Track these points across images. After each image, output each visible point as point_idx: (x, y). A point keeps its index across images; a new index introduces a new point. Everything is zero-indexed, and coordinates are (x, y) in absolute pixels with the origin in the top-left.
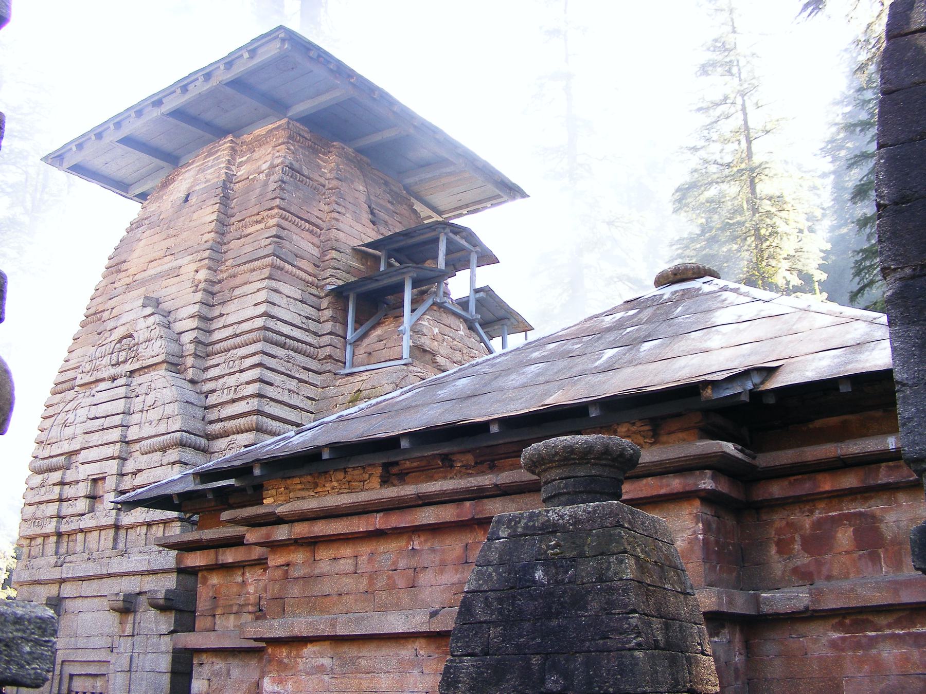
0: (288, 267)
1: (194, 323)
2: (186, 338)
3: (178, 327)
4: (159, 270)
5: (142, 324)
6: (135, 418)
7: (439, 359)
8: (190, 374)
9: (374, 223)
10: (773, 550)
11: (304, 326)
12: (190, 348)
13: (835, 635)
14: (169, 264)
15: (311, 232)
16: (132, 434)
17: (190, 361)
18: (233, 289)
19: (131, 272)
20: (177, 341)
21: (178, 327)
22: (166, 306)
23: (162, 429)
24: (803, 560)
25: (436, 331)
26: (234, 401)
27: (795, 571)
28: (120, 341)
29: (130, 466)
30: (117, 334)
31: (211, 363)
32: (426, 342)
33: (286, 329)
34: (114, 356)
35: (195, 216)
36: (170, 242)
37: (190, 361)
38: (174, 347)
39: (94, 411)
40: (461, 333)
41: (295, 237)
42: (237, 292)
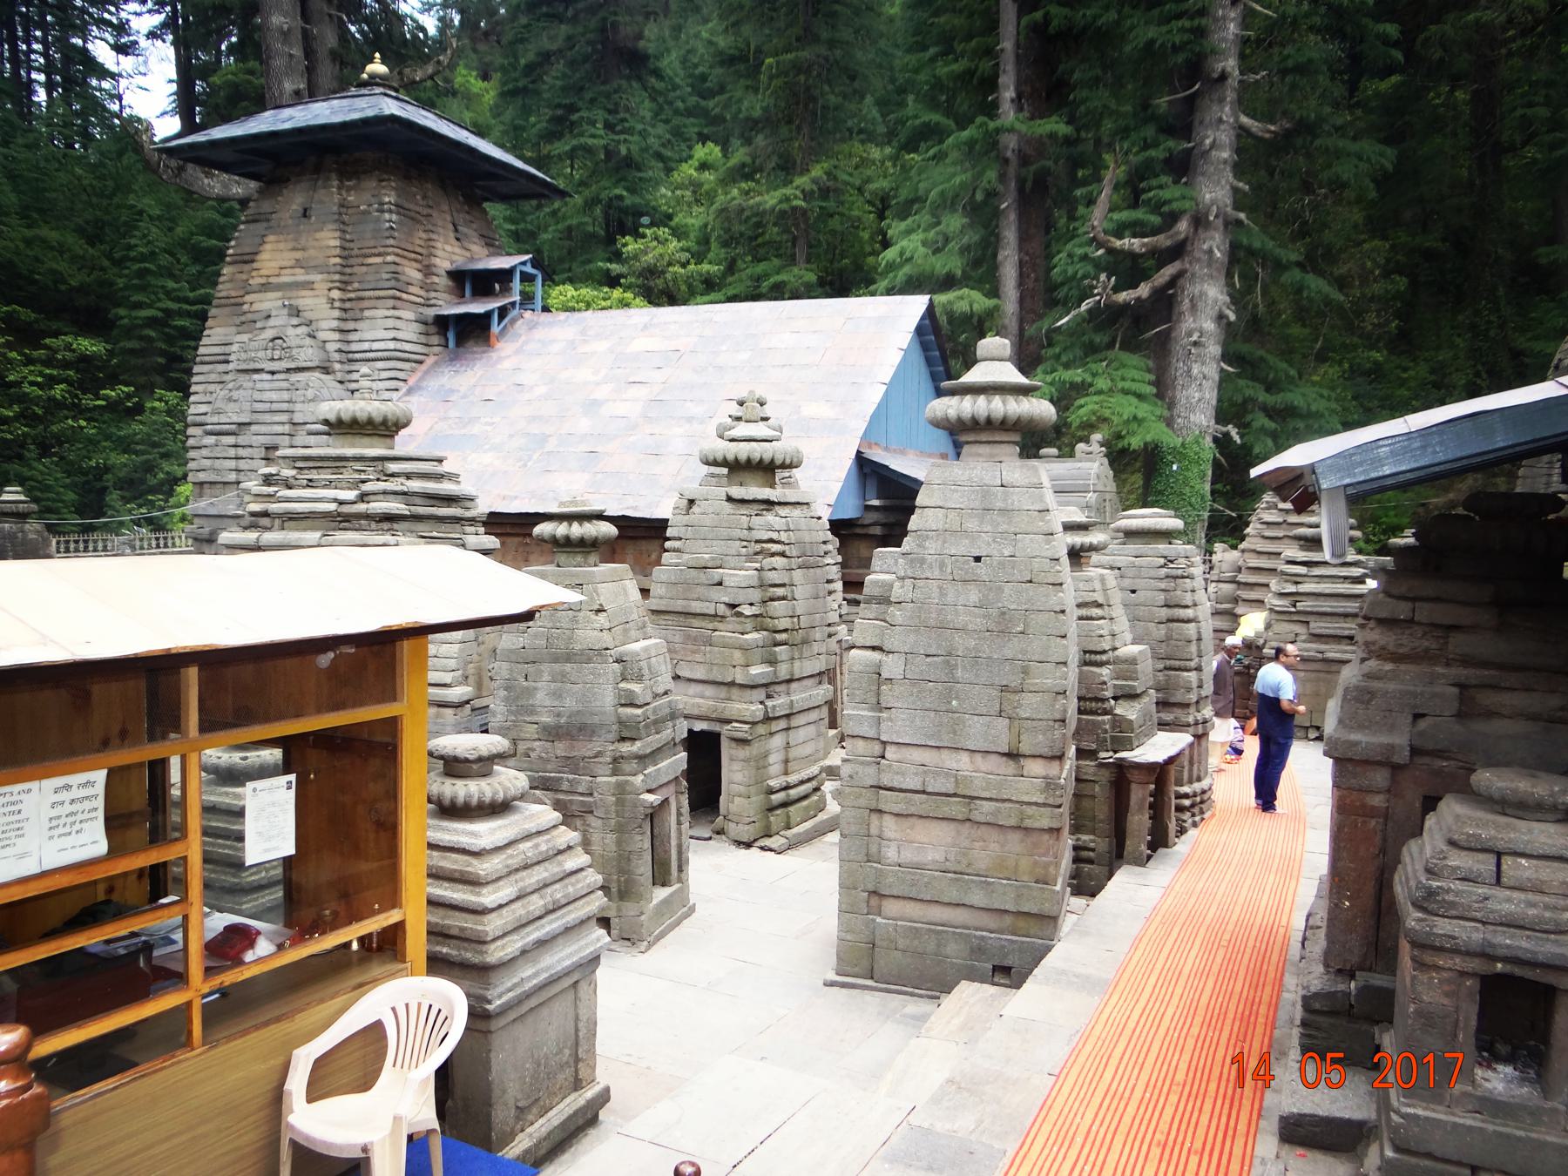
0: (404, 296)
1: (336, 336)
2: (331, 347)
3: (322, 335)
5: (291, 332)
6: (298, 407)
8: (339, 376)
9: (458, 239)
12: (337, 356)
14: (301, 276)
15: (416, 260)
16: (298, 418)
17: (337, 366)
18: (362, 310)
19: (263, 272)
20: (323, 348)
21: (322, 335)
22: (308, 315)
28: (273, 340)
29: (298, 440)
30: (269, 334)
33: (408, 347)
34: (269, 352)
35: (318, 235)
36: (299, 255)
37: (337, 366)
38: (322, 355)
39: (257, 396)
42: (367, 313)
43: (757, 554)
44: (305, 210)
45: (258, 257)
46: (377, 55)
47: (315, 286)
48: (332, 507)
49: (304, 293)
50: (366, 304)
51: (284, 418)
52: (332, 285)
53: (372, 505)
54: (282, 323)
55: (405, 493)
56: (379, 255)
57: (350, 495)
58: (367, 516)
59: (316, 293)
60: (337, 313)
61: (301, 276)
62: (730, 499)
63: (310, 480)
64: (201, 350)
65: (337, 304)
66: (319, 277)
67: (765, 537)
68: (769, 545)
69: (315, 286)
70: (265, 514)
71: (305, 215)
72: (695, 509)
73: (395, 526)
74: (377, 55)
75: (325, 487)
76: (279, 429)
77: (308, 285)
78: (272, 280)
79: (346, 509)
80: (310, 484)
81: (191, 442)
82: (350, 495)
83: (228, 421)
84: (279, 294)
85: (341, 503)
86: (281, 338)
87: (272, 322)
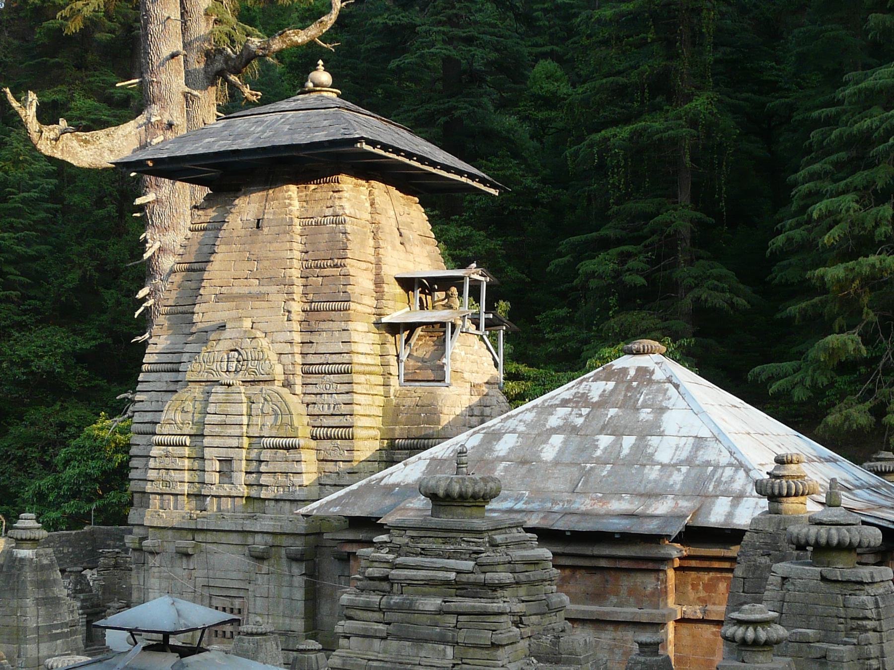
4: (246, 290)
7: (466, 375)
10: (690, 587)
11: (372, 352)
13: (714, 630)
19: (217, 282)
24: (702, 594)
25: (463, 353)
26: (332, 415)
27: (699, 598)
30: (224, 345)
31: (309, 381)
32: (458, 366)
40: (476, 347)
41: (360, 280)
42: (323, 326)
43: (852, 629)
44: (259, 220)
45: (209, 267)
46: (320, 62)
47: (271, 297)
48: (452, 576)
49: (258, 304)
50: (323, 315)
53: (489, 575)
55: (509, 563)
56: (336, 266)
57: (469, 565)
58: (484, 585)
61: (254, 286)
62: (824, 579)
63: (423, 549)
66: (275, 288)
67: (861, 615)
68: (865, 622)
69: (271, 297)
70: (385, 579)
71: (258, 227)
72: (788, 586)
73: (506, 593)
74: (320, 62)
75: (439, 556)
76: (234, 442)
77: (260, 297)
78: (224, 290)
79: (464, 578)
80: (424, 552)
81: (134, 451)
82: (469, 565)
83: (179, 432)
85: (459, 572)
86: (236, 350)
87: (227, 334)
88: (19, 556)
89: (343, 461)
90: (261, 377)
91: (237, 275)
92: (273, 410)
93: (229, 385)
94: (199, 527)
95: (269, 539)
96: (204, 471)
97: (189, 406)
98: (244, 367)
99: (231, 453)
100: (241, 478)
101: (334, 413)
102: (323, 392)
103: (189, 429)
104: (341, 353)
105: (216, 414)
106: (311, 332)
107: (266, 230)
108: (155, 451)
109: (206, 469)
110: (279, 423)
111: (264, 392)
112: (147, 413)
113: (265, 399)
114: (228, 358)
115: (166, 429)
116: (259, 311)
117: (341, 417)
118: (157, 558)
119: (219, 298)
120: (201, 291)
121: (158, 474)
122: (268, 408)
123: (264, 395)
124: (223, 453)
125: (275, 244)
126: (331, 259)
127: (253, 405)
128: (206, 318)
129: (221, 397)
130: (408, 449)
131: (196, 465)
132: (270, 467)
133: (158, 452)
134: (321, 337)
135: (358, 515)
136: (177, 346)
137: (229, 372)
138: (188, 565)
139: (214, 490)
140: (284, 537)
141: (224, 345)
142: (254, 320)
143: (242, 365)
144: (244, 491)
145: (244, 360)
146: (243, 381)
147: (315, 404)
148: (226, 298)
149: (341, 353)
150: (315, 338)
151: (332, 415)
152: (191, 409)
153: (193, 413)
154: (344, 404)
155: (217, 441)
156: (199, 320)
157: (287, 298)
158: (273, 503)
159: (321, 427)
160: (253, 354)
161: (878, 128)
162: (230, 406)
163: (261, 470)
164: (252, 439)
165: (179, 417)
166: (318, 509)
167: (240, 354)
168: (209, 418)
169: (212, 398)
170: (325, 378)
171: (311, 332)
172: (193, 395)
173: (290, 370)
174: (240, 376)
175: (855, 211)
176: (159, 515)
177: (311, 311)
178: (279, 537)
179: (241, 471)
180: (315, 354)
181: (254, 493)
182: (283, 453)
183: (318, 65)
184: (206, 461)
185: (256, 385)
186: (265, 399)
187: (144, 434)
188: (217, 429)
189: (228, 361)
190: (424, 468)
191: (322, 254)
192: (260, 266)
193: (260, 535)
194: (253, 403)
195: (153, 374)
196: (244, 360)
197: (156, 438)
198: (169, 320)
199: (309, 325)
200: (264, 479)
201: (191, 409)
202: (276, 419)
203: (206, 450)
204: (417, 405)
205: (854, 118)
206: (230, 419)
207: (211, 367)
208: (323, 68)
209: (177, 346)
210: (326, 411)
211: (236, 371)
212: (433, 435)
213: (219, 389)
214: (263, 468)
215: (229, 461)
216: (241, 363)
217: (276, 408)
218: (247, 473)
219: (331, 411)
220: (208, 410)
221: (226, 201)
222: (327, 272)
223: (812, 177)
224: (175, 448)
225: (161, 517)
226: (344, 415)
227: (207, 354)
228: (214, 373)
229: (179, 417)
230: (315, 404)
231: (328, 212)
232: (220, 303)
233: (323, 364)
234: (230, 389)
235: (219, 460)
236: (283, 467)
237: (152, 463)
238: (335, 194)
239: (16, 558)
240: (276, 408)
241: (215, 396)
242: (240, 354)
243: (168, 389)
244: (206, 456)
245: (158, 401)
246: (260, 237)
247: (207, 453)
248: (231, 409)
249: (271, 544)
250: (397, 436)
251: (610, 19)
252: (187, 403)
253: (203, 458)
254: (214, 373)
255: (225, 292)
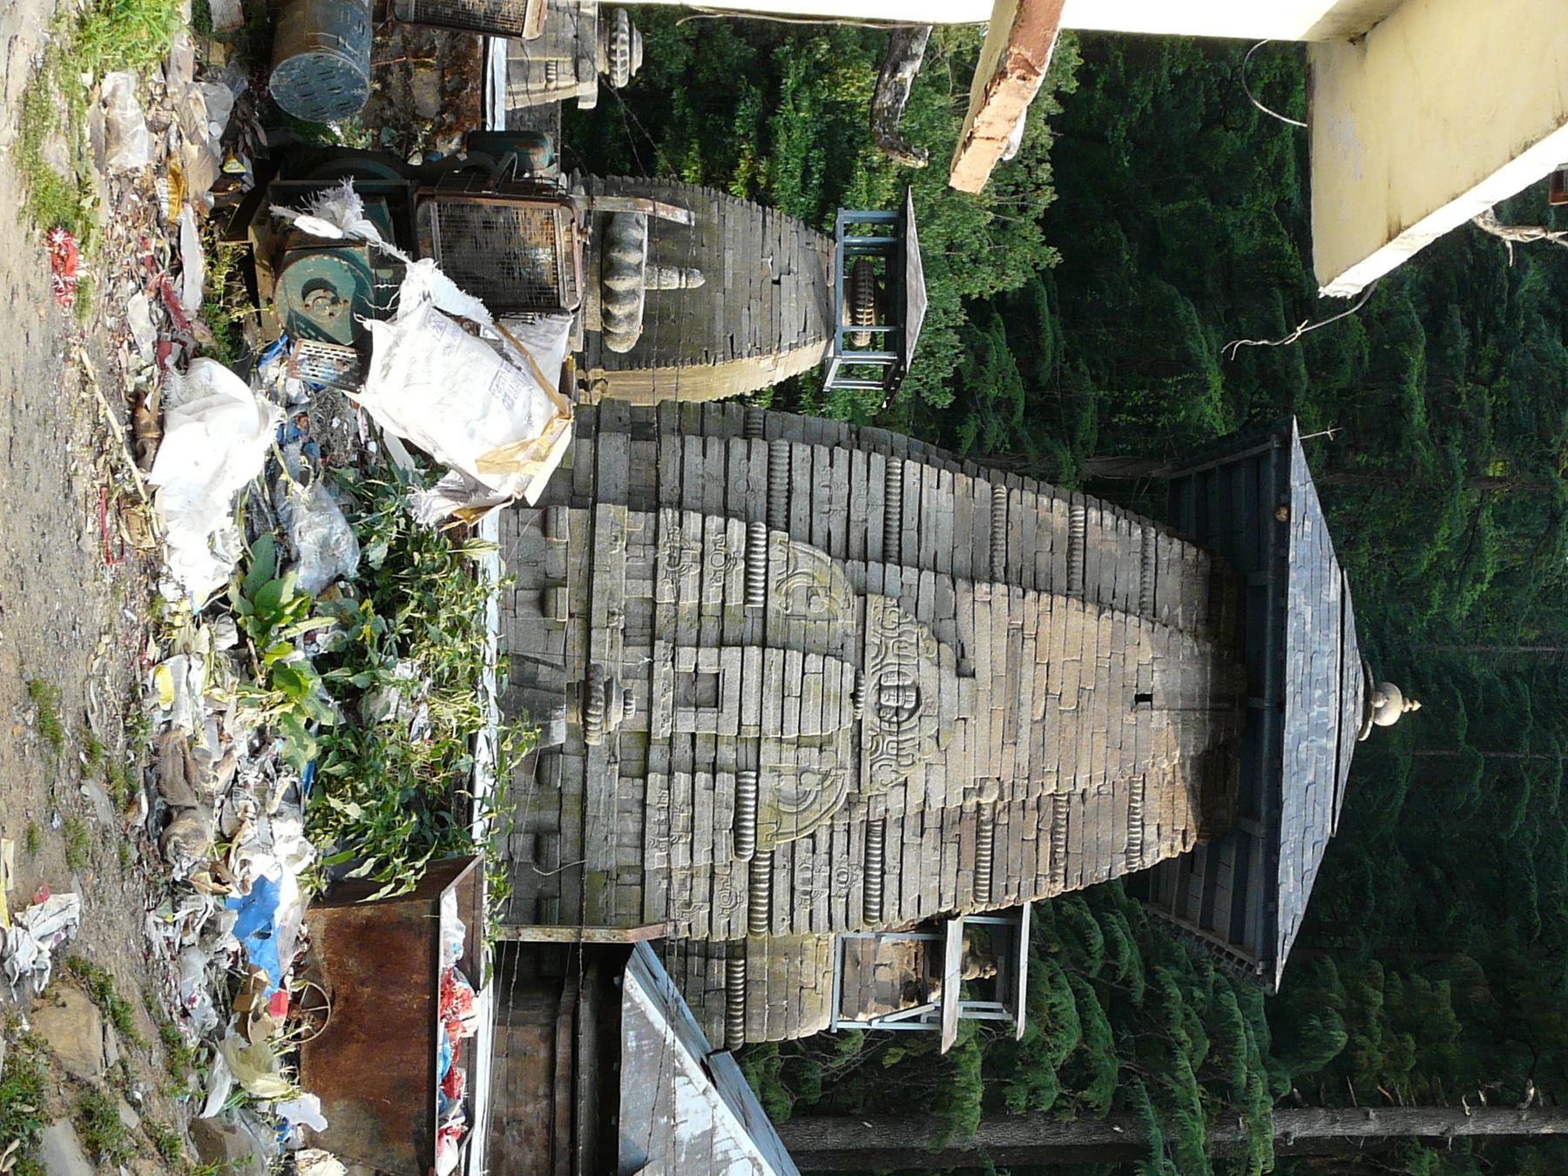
4: (1026, 697)
19: (1045, 629)
23: (765, 814)
26: (793, 889)
30: (928, 676)
42: (951, 850)
44: (1148, 698)
46: (1417, 706)
47: (1009, 750)
49: (999, 723)
50: (968, 849)
51: (770, 724)
52: (1007, 792)
54: (946, 706)
59: (996, 754)
60: (954, 803)
61: (1031, 711)
64: (912, 467)
65: (971, 802)
66: (1024, 758)
69: (1009, 750)
71: (1141, 698)
76: (750, 718)
77: (1011, 735)
83: (772, 585)
84: (1002, 670)
87: (950, 681)
88: (553, 723)
89: (710, 913)
90: (866, 764)
91: (1056, 670)
92: (806, 794)
93: (854, 696)
94: (594, 633)
95: (573, 788)
96: (698, 645)
97: (819, 606)
98: (885, 726)
99: (730, 708)
100: (687, 723)
101: (797, 894)
102: (834, 868)
103: (777, 607)
104: (900, 899)
105: (803, 674)
106: (941, 827)
107: (1131, 719)
108: (737, 529)
109: (701, 650)
110: (783, 808)
111: (840, 772)
112: (807, 477)
113: (826, 776)
114: (904, 688)
115: (777, 554)
116: (986, 728)
117: (787, 908)
118: (537, 532)
119: (1017, 634)
120: (1031, 595)
121: (695, 540)
122: (810, 781)
123: (833, 773)
124: (730, 691)
125: (1103, 743)
126: (1067, 852)
127: (817, 750)
128: (982, 611)
129: (833, 685)
130: (727, 983)
131: (711, 629)
132: (703, 795)
133: (735, 537)
134: (931, 850)
135: (623, 1094)
136: (932, 537)
137: (879, 710)
138: (522, 603)
139: (662, 670)
140: (577, 820)
141: (928, 676)
142: (971, 721)
143: (890, 722)
144: (661, 731)
145: (899, 724)
146: (860, 721)
147: (814, 852)
148: (1014, 654)
149: (900, 899)
150: (931, 837)
151: (793, 889)
152: (815, 610)
153: (805, 617)
154: (811, 911)
155: (752, 678)
156: (978, 596)
157: (1006, 785)
158: (640, 797)
159: (772, 867)
160: (910, 743)
161: (1178, 1081)
162: (815, 705)
163: (698, 774)
164: (755, 744)
165: (799, 582)
166: (635, 1006)
167: (912, 712)
168: (795, 657)
169: (832, 663)
170: (858, 872)
171: (941, 827)
172: (840, 613)
173: (875, 808)
174: (869, 719)
175: (1053, 1060)
176: (616, 540)
177: (979, 823)
178: (578, 808)
179: (697, 728)
180: (902, 844)
181: (657, 756)
182: (728, 823)
183: (1412, 702)
184: (716, 650)
185: (853, 748)
186: (826, 776)
187: (770, 470)
188: (774, 677)
189: (898, 687)
190: (697, 1133)
191: (1076, 835)
192: (1067, 718)
193: (580, 767)
194: (821, 751)
195: (882, 486)
196: (899, 724)
197: (762, 528)
198: (980, 512)
199: (954, 823)
200: (682, 779)
201: (815, 610)
202: (788, 801)
203: (736, 651)
204: (802, 988)
205: (1194, 1014)
206: (792, 704)
207: (890, 654)
208: (1406, 710)
209: (932, 537)
210: (799, 876)
211: (880, 708)
212: (751, 1030)
213: (849, 677)
214: (703, 778)
215: (716, 702)
216: (895, 719)
217: (811, 798)
218: (693, 735)
219: (799, 888)
220: (811, 657)
221: (1191, 604)
222: (1045, 847)
223: (1112, 947)
224: (742, 578)
225: (612, 545)
226: (792, 914)
227: (915, 641)
228: (878, 660)
229: (799, 582)
230: (814, 852)
231: (1151, 830)
232: (1005, 640)
233: (883, 862)
234: (847, 701)
235: (718, 674)
236: (704, 824)
237: (715, 522)
238: (1180, 837)
239: (549, 718)
240: (811, 798)
241: (836, 669)
242: (912, 712)
243: (852, 524)
244: (726, 651)
245: (830, 501)
246: (1119, 708)
247: (731, 654)
248: (811, 706)
249: (565, 790)
250: (749, 960)
251: (1403, 391)
252: (826, 601)
253: (721, 643)
254: (878, 660)
255: (1026, 651)
